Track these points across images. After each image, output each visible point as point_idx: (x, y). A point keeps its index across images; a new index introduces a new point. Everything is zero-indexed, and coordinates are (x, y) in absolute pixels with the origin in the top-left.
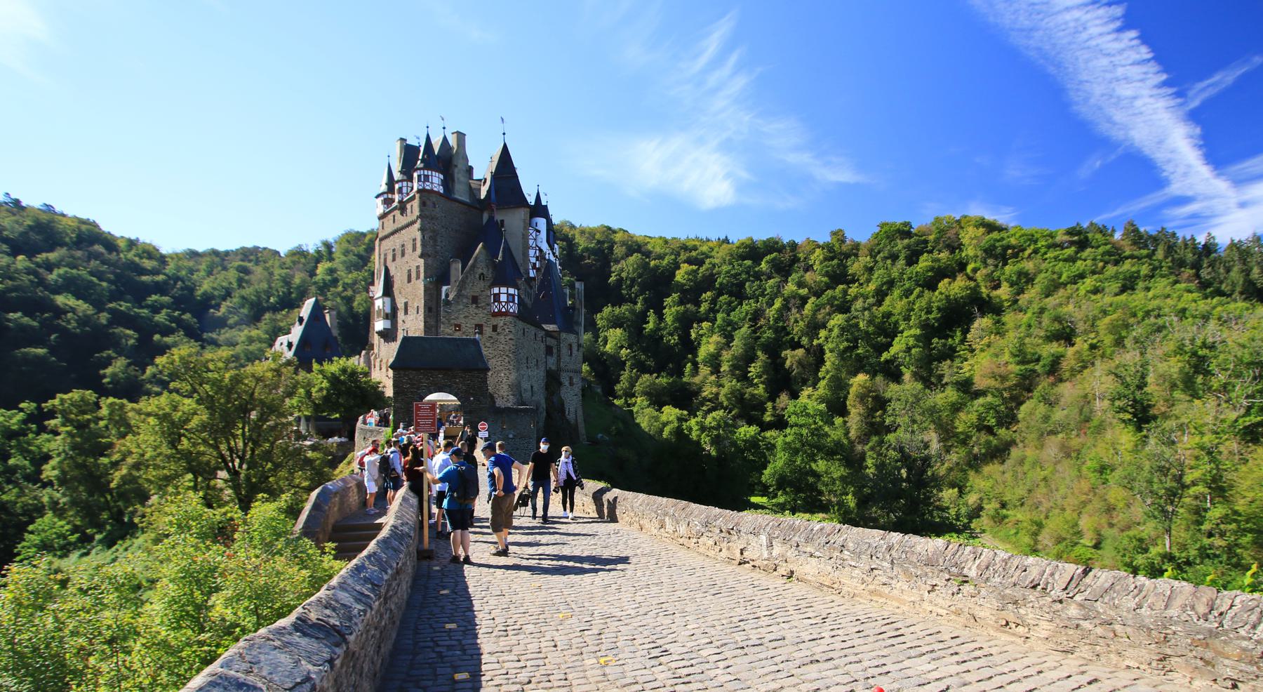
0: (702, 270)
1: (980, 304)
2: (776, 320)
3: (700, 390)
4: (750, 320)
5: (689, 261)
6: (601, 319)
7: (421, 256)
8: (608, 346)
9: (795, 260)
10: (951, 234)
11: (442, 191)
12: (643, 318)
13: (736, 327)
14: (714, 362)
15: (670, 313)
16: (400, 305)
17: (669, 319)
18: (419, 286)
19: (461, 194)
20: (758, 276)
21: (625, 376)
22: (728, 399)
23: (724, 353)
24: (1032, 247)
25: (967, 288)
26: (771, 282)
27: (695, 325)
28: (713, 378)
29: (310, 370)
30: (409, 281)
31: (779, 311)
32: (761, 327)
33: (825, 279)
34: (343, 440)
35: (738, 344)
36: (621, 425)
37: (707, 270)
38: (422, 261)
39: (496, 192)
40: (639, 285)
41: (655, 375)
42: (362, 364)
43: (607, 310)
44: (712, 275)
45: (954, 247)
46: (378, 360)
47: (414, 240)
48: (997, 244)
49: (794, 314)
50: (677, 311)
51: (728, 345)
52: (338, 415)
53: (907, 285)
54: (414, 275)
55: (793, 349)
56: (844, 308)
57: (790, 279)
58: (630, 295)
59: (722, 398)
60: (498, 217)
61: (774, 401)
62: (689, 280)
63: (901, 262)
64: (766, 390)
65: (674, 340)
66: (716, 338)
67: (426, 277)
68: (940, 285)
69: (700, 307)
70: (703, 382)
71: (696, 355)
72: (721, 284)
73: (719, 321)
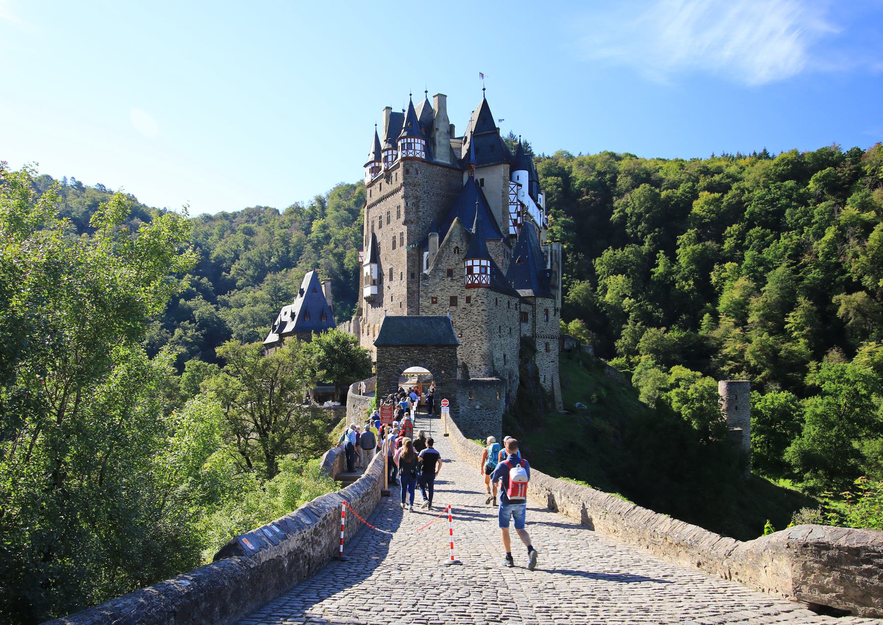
0: (726, 198)
2: (827, 256)
3: (720, 345)
4: (790, 257)
5: (711, 188)
6: (599, 265)
7: (405, 223)
8: (608, 296)
11: (424, 157)
12: (651, 260)
14: (740, 312)
15: (684, 254)
16: (386, 272)
17: (683, 260)
18: (403, 252)
19: (442, 157)
20: (803, 200)
21: (628, 330)
23: (753, 299)
27: (716, 267)
28: (738, 331)
29: (309, 340)
30: (394, 248)
31: (832, 243)
32: (805, 265)
34: (337, 404)
35: (771, 289)
36: (603, 392)
37: (734, 197)
38: (405, 228)
39: (477, 150)
40: (647, 222)
41: (663, 329)
42: (352, 334)
43: (607, 254)
44: (740, 203)
46: (366, 325)
47: (399, 207)
50: (694, 251)
52: (332, 381)
54: (398, 242)
55: (850, 292)
58: (636, 234)
59: (748, 356)
60: (478, 176)
61: (820, 360)
62: (710, 211)
65: (688, 285)
66: (742, 281)
67: (408, 245)
69: (723, 243)
70: (725, 336)
71: (716, 303)
72: (752, 214)
73: (747, 261)
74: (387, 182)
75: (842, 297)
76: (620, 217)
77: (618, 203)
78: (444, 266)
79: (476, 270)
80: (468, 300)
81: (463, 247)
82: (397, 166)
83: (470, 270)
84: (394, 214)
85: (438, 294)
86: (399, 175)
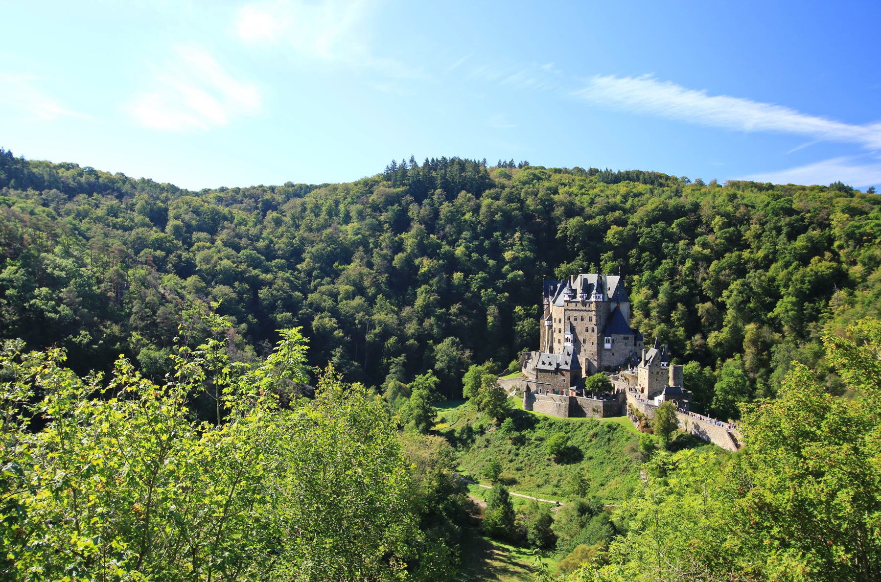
1: (840, 279)
9: (698, 222)
10: (823, 214)
13: (660, 282)
18: (594, 336)
25: (830, 268)
26: (682, 242)
28: (646, 321)
35: (662, 298)
40: (580, 242)
44: (635, 234)
45: (824, 225)
48: (857, 231)
51: (655, 295)
53: (788, 258)
54: (590, 330)
56: (740, 270)
57: (696, 241)
61: (690, 339)
64: (685, 331)
66: (644, 290)
67: (598, 334)
68: (812, 260)
72: (643, 243)
74: (583, 305)
75: (700, 305)
77: (561, 226)
78: (655, 363)
81: (660, 358)
82: (592, 303)
83: (663, 365)
86: (593, 307)
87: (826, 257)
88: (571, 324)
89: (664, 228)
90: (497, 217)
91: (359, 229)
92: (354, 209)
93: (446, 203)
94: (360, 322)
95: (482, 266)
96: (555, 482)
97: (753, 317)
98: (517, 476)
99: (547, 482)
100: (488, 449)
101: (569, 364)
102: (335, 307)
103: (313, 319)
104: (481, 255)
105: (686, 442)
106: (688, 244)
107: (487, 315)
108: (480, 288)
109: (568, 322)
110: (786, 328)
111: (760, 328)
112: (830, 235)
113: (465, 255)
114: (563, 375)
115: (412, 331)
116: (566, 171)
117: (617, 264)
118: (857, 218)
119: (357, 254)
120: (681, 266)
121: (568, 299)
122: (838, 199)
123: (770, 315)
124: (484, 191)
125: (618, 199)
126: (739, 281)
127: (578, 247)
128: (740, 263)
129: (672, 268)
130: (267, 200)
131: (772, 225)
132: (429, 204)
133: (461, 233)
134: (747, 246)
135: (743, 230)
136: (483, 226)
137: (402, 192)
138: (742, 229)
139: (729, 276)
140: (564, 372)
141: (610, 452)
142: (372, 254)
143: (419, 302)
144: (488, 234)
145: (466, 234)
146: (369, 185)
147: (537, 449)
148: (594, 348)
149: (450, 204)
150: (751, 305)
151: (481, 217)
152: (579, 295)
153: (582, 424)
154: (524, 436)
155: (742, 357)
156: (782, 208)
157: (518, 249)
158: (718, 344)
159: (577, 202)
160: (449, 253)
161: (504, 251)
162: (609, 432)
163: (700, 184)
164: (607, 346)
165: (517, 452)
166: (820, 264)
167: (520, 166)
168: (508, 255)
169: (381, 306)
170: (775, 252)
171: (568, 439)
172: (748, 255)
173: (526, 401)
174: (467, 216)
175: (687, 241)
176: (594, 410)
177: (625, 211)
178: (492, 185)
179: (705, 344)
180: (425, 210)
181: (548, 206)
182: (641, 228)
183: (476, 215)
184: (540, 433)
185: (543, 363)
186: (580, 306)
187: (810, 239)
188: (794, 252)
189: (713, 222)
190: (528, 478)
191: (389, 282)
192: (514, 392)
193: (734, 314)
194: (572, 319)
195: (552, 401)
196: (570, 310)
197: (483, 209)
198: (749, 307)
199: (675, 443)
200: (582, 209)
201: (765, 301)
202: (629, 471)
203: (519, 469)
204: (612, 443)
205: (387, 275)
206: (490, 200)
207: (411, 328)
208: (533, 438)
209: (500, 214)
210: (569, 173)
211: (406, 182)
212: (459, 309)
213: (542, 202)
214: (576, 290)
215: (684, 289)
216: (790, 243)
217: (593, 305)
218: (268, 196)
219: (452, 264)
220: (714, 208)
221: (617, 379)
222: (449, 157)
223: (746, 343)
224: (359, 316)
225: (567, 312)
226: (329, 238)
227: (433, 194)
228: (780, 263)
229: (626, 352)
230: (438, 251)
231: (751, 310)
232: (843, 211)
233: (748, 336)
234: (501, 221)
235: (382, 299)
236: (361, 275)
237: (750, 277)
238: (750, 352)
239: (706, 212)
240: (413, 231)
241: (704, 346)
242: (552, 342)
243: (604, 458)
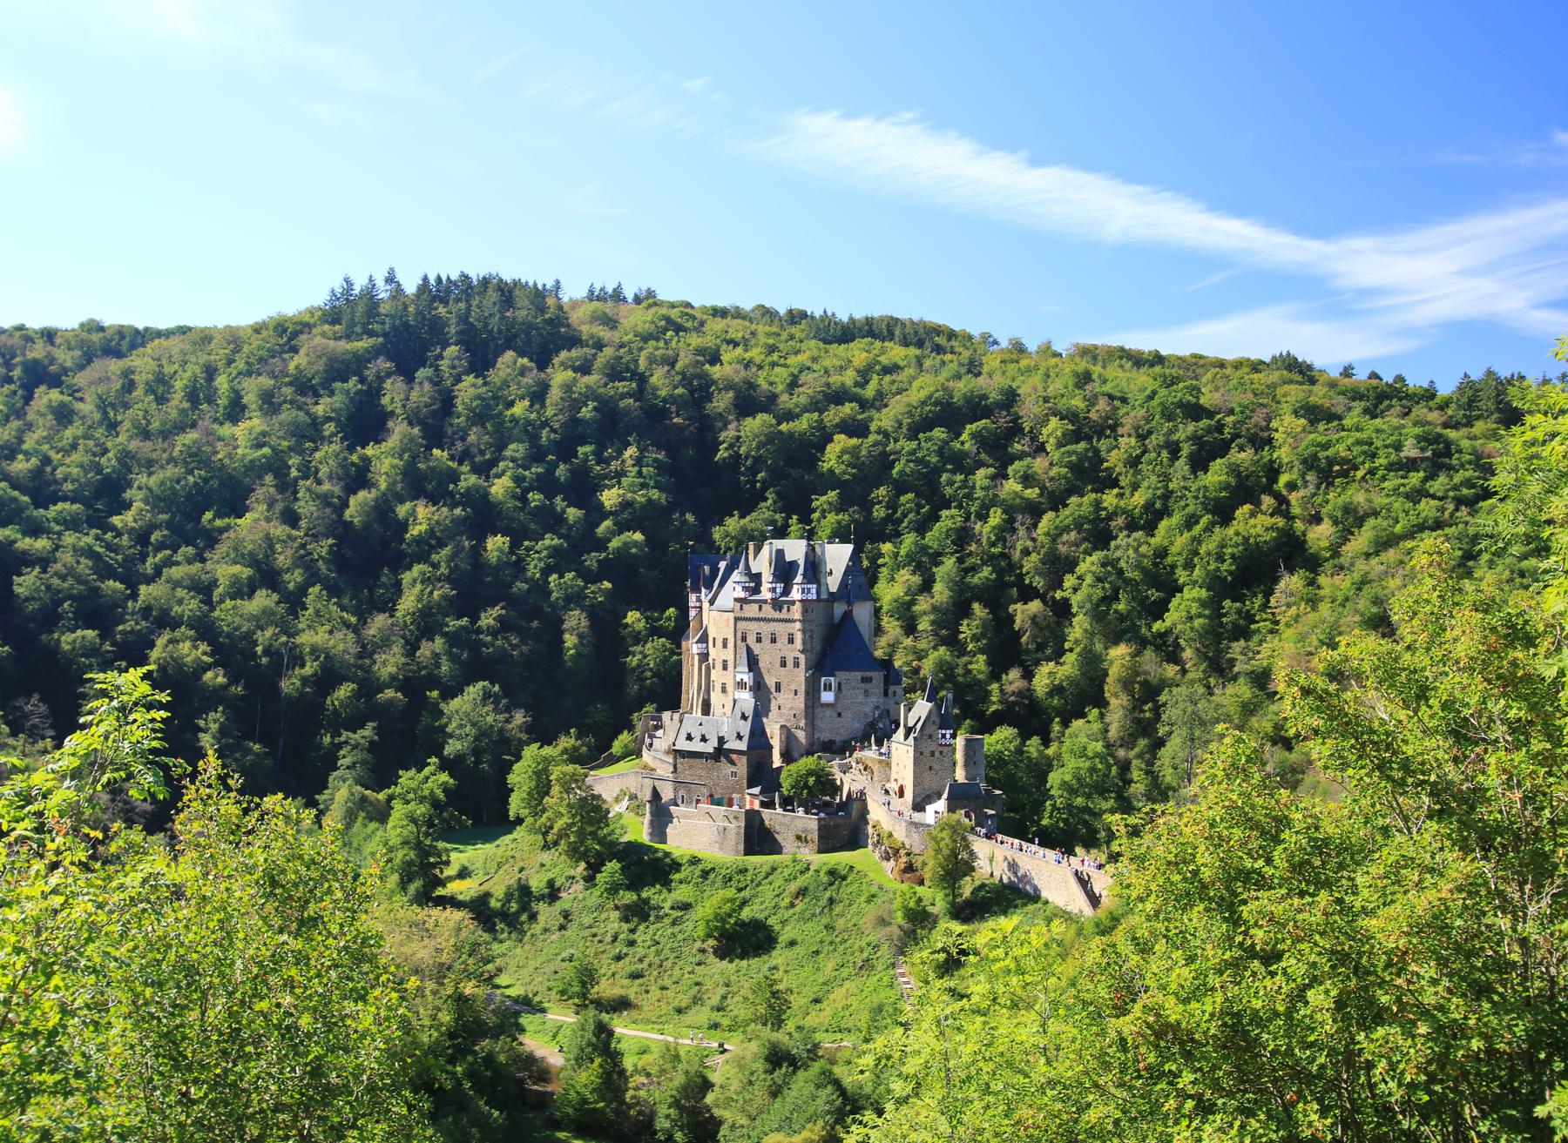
9: (1015, 430)
10: (1258, 418)
13: (936, 557)
18: (799, 677)
22: (935, 674)
24: (1367, 466)
28: (908, 642)
32: (970, 554)
33: (1064, 470)
35: (941, 592)
40: (768, 469)
44: (884, 454)
45: (1261, 441)
49: (1021, 541)
51: (927, 586)
53: (1190, 509)
54: (790, 663)
56: (1099, 534)
57: (1010, 470)
58: (754, 485)
61: (999, 679)
63: (1182, 465)
64: (989, 663)
67: (807, 671)
68: (1238, 513)
72: (901, 473)
74: (774, 608)
75: (1019, 606)
76: (731, 456)
77: (728, 434)
78: (926, 732)
79: (948, 736)
80: (941, 753)
81: (938, 721)
82: (793, 603)
83: (944, 736)
84: (783, 639)
85: (923, 749)
87: (1264, 507)
88: (749, 649)
89: (946, 443)
90: (586, 412)
91: (264, 434)
92: (252, 389)
93: (470, 379)
94: (267, 652)
95: (553, 521)
96: (715, 1001)
97: (1124, 632)
98: (632, 991)
99: (696, 1000)
100: (568, 933)
101: (746, 739)
102: (206, 616)
103: (152, 645)
104: (550, 496)
105: (991, 898)
106: (993, 478)
107: (562, 633)
108: (547, 572)
109: (742, 646)
110: (1188, 654)
111: (1138, 653)
112: (1272, 462)
113: (515, 497)
114: (733, 763)
115: (391, 669)
116: (738, 314)
117: (846, 517)
118: (1321, 427)
119: (260, 493)
120: (979, 524)
121: (742, 595)
122: (1286, 388)
123: (1158, 626)
124: (557, 352)
125: (849, 378)
126: (1097, 556)
127: (763, 481)
128: (1098, 519)
129: (963, 529)
130: (36, 362)
131: (1162, 438)
132: (430, 380)
133: (506, 446)
134: (1114, 483)
135: (1103, 448)
136: (554, 431)
137: (366, 350)
138: (1103, 445)
139: (1077, 545)
140: (734, 756)
141: (833, 928)
142: (295, 492)
143: (408, 603)
144: (565, 450)
145: (515, 449)
146: (288, 333)
147: (677, 929)
148: (800, 703)
149: (480, 381)
150: (1122, 607)
151: (549, 412)
152: (765, 586)
153: (774, 869)
154: (646, 901)
155: (1102, 716)
156: (1180, 405)
157: (632, 485)
158: (1057, 690)
159: (762, 382)
160: (477, 491)
161: (598, 488)
162: (831, 884)
163: (1019, 348)
164: (827, 697)
165: (632, 936)
166: (1252, 521)
167: (638, 300)
168: (610, 497)
169: (317, 613)
170: (1167, 495)
171: (744, 903)
172: (1115, 501)
173: (652, 823)
174: (519, 409)
175: (992, 470)
176: (799, 838)
177: (864, 404)
178: (574, 341)
179: (1029, 690)
180: (421, 393)
181: (699, 389)
182: (896, 440)
183: (537, 406)
184: (682, 893)
185: (689, 738)
186: (768, 611)
187: (1234, 470)
188: (1204, 496)
189: (1044, 431)
190: (655, 993)
191: (336, 558)
192: (625, 803)
193: (1086, 626)
194: (751, 640)
195: (707, 822)
196: (746, 619)
197: (555, 394)
198: (1116, 611)
199: (968, 903)
200: (773, 398)
201: (1147, 597)
202: (873, 967)
203: (635, 976)
204: (838, 909)
205: (331, 541)
206: (570, 373)
207: (389, 663)
208: (668, 905)
209: (591, 405)
210: (744, 318)
211: (377, 327)
212: (499, 619)
213: (686, 380)
214: (759, 575)
215: (986, 572)
216: (1196, 477)
217: (797, 608)
218: (38, 352)
219: (484, 517)
220: (1046, 400)
221: (845, 769)
222: (476, 272)
223: (1111, 686)
224: (264, 636)
225: (739, 623)
226: (191, 455)
227: (440, 357)
228: (1176, 519)
229: (868, 709)
230: (451, 486)
231: (1121, 617)
232: (1296, 413)
233: (1114, 672)
234: (594, 420)
235: (319, 597)
236: (269, 541)
237: (1117, 547)
238: (1118, 704)
239: (1029, 409)
240: (393, 441)
241: (1027, 693)
242: (708, 691)
243: (822, 942)
